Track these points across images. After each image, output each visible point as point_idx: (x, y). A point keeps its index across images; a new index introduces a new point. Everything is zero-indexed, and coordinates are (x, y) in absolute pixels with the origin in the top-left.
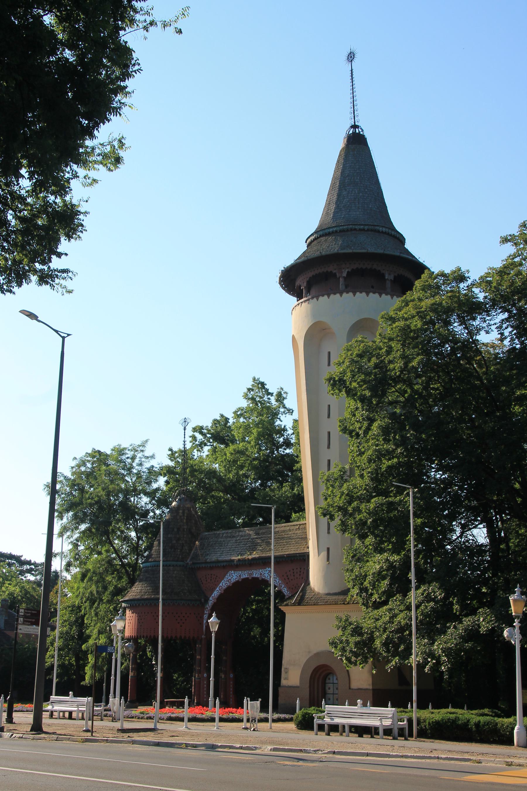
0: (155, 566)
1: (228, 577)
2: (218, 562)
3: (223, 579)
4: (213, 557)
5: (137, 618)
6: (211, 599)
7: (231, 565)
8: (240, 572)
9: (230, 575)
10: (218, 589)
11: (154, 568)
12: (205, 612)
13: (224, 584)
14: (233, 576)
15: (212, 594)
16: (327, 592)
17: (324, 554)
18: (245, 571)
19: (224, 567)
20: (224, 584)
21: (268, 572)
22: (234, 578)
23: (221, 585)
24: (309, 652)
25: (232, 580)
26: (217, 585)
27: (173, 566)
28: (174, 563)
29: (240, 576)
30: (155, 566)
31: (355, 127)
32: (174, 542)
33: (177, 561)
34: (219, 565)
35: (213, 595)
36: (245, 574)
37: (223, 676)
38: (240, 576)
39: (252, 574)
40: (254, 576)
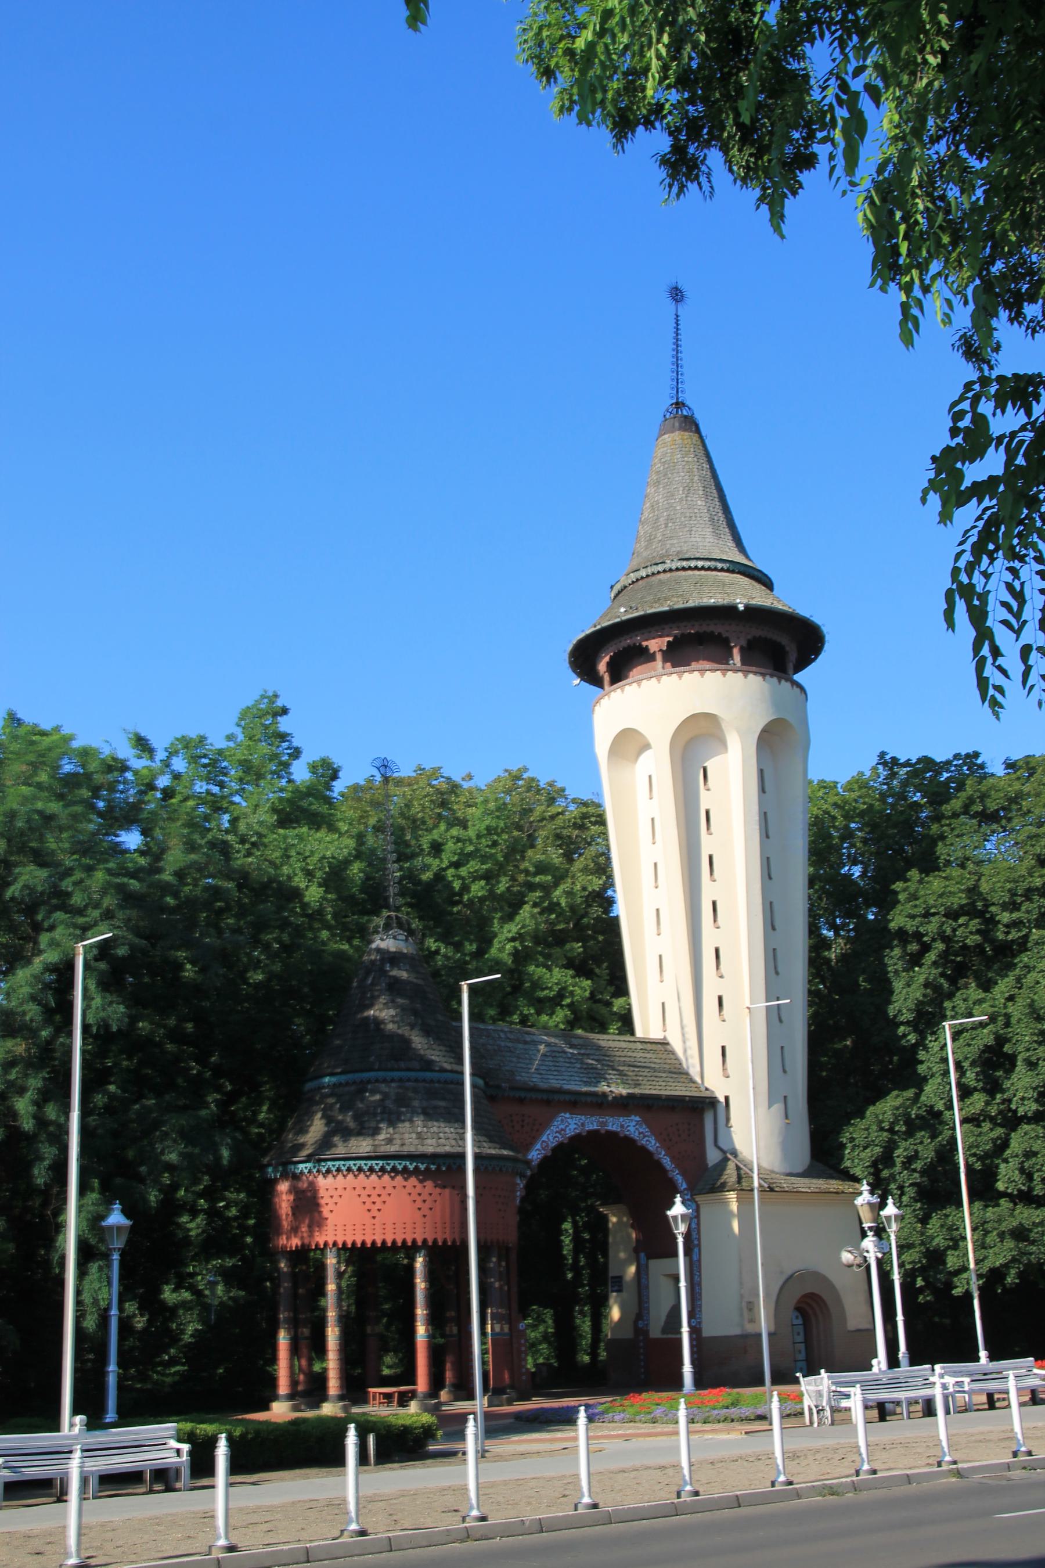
1: (557, 1124)
2: (560, 1091)
7: (576, 1102)
8: (583, 1117)
9: (562, 1121)
10: (538, 1146)
11: (452, 1086)
13: (551, 1138)
14: (568, 1125)
16: (788, 1171)
17: (778, 1107)
18: (592, 1115)
19: (548, 1102)
20: (551, 1138)
21: (634, 1123)
22: (572, 1127)
23: (544, 1138)
24: (782, 1273)
26: (534, 1139)
29: (583, 1125)
31: (679, 405)
36: (592, 1124)
38: (583, 1125)
39: (604, 1124)
40: (610, 1128)
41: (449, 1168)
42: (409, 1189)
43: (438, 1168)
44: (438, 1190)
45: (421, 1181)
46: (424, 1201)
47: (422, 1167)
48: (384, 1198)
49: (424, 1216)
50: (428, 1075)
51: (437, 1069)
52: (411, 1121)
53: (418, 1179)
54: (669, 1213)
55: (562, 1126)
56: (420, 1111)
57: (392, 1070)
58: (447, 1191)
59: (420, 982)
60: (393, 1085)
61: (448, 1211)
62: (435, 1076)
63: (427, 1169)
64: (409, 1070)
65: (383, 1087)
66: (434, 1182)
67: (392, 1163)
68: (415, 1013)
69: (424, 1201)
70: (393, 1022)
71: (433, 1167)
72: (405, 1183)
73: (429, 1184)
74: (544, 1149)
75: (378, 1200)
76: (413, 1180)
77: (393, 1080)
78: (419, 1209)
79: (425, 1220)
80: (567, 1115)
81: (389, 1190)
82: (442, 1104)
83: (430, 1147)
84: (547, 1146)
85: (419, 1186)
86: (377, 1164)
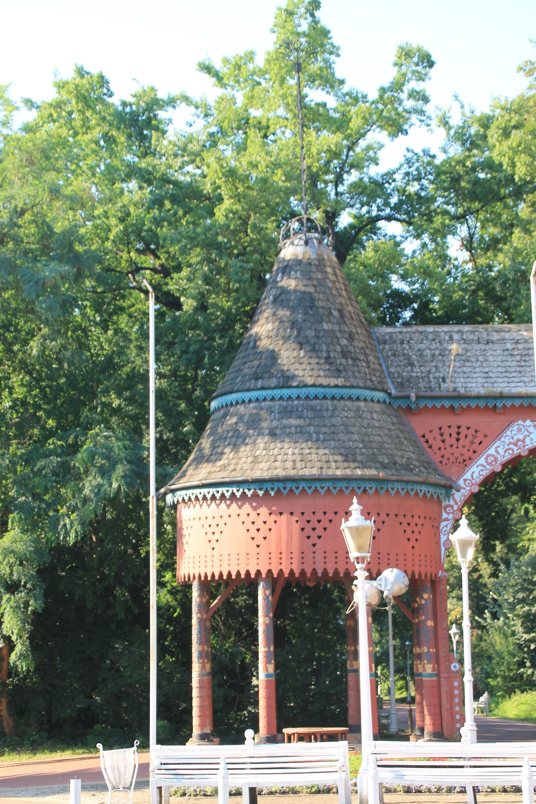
0: (316, 398)
3: (498, 436)
4: (477, 386)
5: (296, 527)
6: (461, 482)
9: (519, 430)
10: (482, 461)
11: (314, 402)
12: (444, 516)
13: (501, 451)
15: (463, 473)
20: (501, 451)
23: (492, 451)
25: (527, 440)
27: (365, 400)
28: (368, 394)
30: (316, 398)
32: (344, 342)
33: (375, 389)
34: (438, 405)
35: (468, 476)
37: (429, 668)
41: (278, 492)
42: (243, 517)
43: (267, 492)
44: (274, 517)
45: (254, 509)
46: (258, 530)
47: (249, 493)
48: (222, 527)
49: (258, 546)
50: (286, 392)
51: (295, 384)
52: (254, 443)
53: (252, 506)
54: (451, 537)
55: (521, 437)
56: (267, 432)
57: (248, 390)
58: (284, 517)
59: (312, 290)
60: (251, 405)
61: (284, 539)
62: (293, 392)
63: (255, 495)
64: (263, 388)
65: (241, 409)
66: (269, 508)
67: (221, 490)
68: (293, 324)
69: (258, 530)
70: (269, 337)
71: (261, 493)
72: (239, 511)
73: (264, 511)
74: (490, 464)
75: (217, 530)
76: (247, 508)
77: (250, 401)
78: (253, 539)
79: (258, 550)
80: (528, 422)
81: (226, 519)
82: (294, 422)
83: (261, 471)
84: (496, 459)
85: (253, 514)
86: (209, 492)
